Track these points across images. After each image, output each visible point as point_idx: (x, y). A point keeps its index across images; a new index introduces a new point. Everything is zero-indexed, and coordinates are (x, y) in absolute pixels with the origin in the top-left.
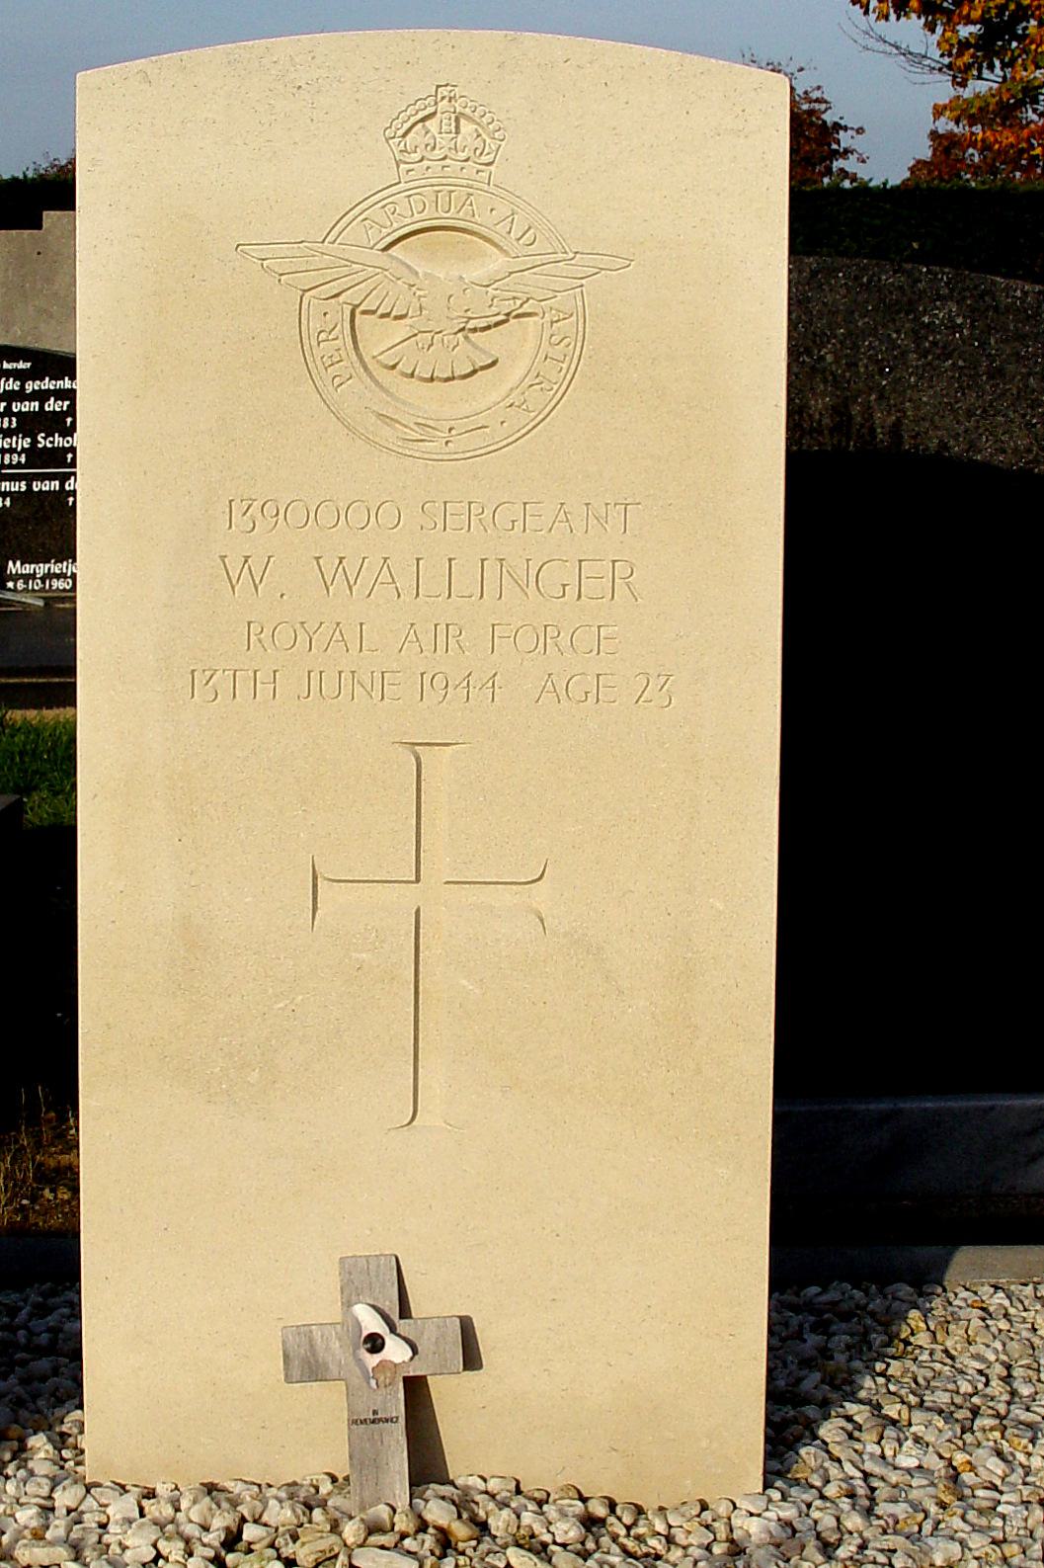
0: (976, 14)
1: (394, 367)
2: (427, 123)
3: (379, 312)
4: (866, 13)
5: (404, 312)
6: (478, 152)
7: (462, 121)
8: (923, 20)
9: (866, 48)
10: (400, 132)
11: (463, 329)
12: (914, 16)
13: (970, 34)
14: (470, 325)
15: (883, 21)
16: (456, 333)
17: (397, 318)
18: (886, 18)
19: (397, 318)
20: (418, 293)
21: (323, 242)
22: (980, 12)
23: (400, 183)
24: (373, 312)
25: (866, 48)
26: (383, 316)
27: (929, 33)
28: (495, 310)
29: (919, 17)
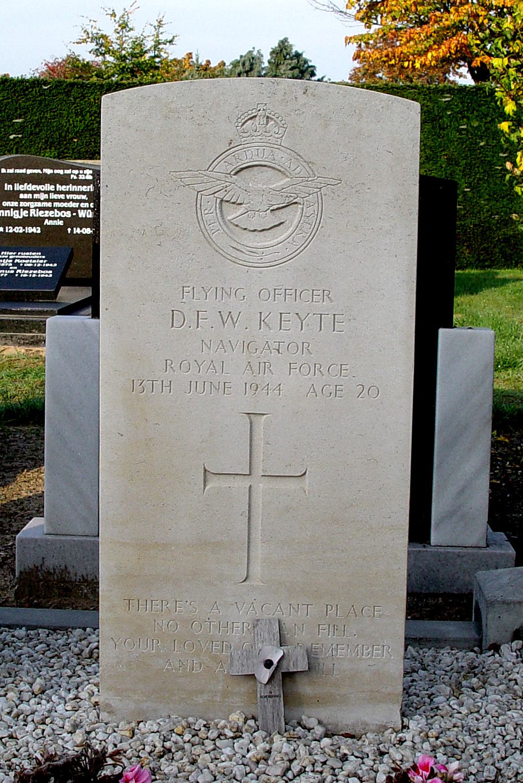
9: (317, 8)
25: (317, 8)
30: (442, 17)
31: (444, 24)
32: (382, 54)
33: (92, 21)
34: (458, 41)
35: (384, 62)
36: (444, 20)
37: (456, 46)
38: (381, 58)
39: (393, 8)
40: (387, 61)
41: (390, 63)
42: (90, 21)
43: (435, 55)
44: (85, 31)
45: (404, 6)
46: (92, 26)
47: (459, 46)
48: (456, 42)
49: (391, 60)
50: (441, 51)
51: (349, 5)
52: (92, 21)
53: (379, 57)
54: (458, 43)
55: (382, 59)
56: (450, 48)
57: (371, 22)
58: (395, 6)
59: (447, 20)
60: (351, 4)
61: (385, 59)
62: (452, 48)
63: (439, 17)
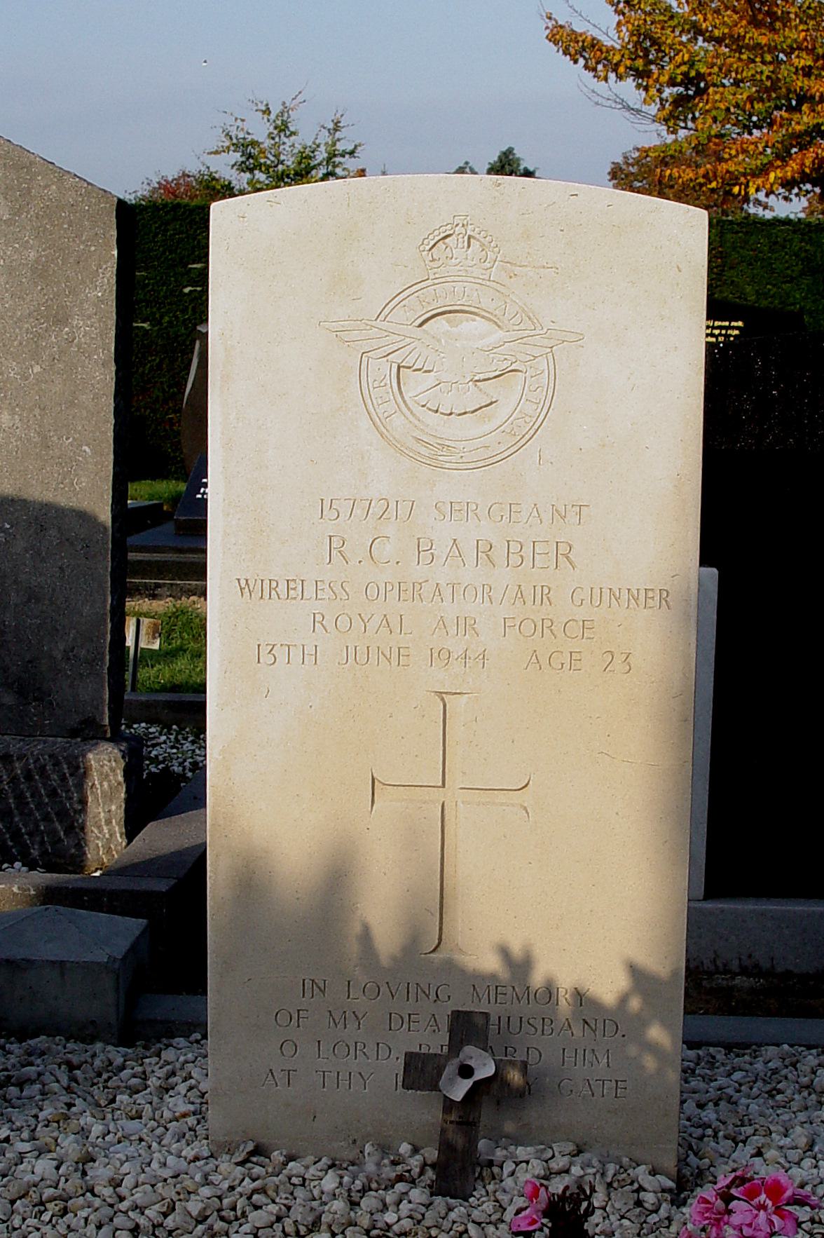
0: (664, 79)
2: (447, 241)
3: (414, 368)
6: (482, 261)
7: (472, 240)
8: (635, 84)
9: (597, 103)
10: (428, 248)
11: (471, 380)
14: (476, 378)
17: (426, 372)
19: (426, 372)
21: (376, 320)
23: (428, 279)
25: (597, 103)
26: (414, 371)
29: (634, 80)
30: (792, 120)
31: (793, 129)
32: (697, 173)
33: (239, 121)
34: (817, 154)
35: (701, 185)
36: (793, 123)
37: (813, 162)
38: (696, 179)
39: (718, 104)
40: (705, 184)
41: (709, 186)
42: (236, 119)
43: (780, 175)
44: (227, 134)
45: (734, 102)
46: (238, 127)
47: (816, 161)
48: (814, 155)
49: (710, 183)
50: (788, 169)
51: (648, 99)
52: (239, 121)
53: (693, 178)
54: (817, 157)
55: (698, 181)
56: (803, 164)
57: (678, 125)
58: (720, 102)
59: (798, 123)
60: (651, 98)
61: (702, 180)
62: (807, 164)
63: (787, 119)
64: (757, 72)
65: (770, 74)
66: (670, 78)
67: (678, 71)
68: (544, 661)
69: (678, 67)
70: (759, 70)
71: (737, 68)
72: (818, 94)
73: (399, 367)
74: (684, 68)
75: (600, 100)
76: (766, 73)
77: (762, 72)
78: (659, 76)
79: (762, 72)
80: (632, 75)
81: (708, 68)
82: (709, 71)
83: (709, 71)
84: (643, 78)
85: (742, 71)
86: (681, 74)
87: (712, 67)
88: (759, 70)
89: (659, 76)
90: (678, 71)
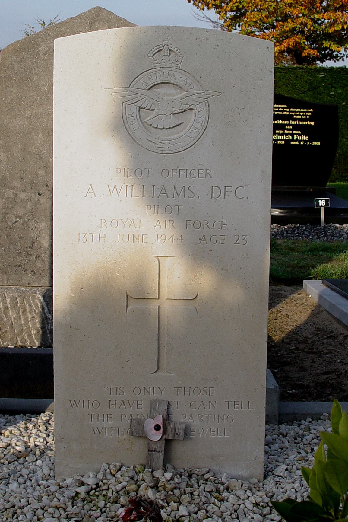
0: (229, 9)
1: (151, 125)
3: (147, 108)
4: (198, 8)
5: (149, 108)
8: (215, 11)
9: (198, 19)
11: (172, 114)
12: (213, 9)
13: (230, 15)
14: (174, 113)
15: (202, 10)
16: (170, 115)
18: (203, 9)
19: (152, 110)
20: (158, 103)
22: (230, 8)
24: (144, 108)
25: (198, 19)
27: (218, 14)
28: (181, 108)
29: (214, 9)
30: (284, 25)
31: (284, 29)
33: (31, 28)
34: (295, 40)
36: (284, 27)
39: (252, 19)
42: (30, 27)
44: (27, 34)
45: (259, 18)
46: (31, 31)
48: (294, 40)
51: (221, 17)
52: (31, 28)
54: (295, 41)
58: (253, 18)
59: (287, 27)
60: (222, 17)
63: (282, 25)
64: (269, 6)
65: (275, 6)
66: (231, 8)
67: (234, 5)
68: (208, 239)
69: (234, 4)
70: (270, 5)
71: (261, 4)
72: (295, 15)
73: (140, 108)
74: (237, 4)
75: (200, 18)
76: (273, 6)
77: (271, 6)
78: (226, 8)
79: (271, 6)
80: (214, 7)
81: (247, 4)
82: (248, 5)
83: (248, 5)
84: (218, 9)
85: (263, 5)
86: (236, 7)
87: (249, 4)
88: (270, 5)
89: (226, 8)
90: (234, 5)
